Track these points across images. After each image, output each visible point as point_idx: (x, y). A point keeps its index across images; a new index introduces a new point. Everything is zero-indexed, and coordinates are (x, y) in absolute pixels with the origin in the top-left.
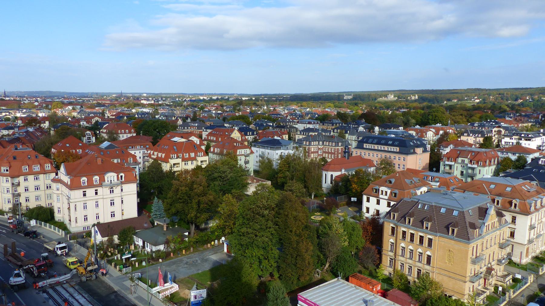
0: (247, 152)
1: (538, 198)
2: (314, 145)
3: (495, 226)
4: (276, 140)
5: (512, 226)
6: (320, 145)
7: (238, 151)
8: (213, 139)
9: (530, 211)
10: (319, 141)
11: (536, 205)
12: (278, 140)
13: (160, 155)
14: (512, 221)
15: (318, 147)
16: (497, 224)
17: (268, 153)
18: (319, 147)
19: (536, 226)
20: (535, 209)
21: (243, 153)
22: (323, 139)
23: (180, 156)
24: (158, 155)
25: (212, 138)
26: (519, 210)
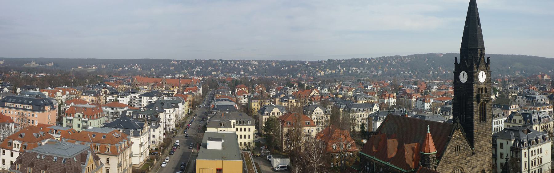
1: (122, 142)
3: (93, 168)
5: (108, 166)
9: (117, 153)
11: (121, 148)
14: (107, 162)
16: (94, 167)
19: (122, 163)
20: (121, 150)
26: (111, 153)
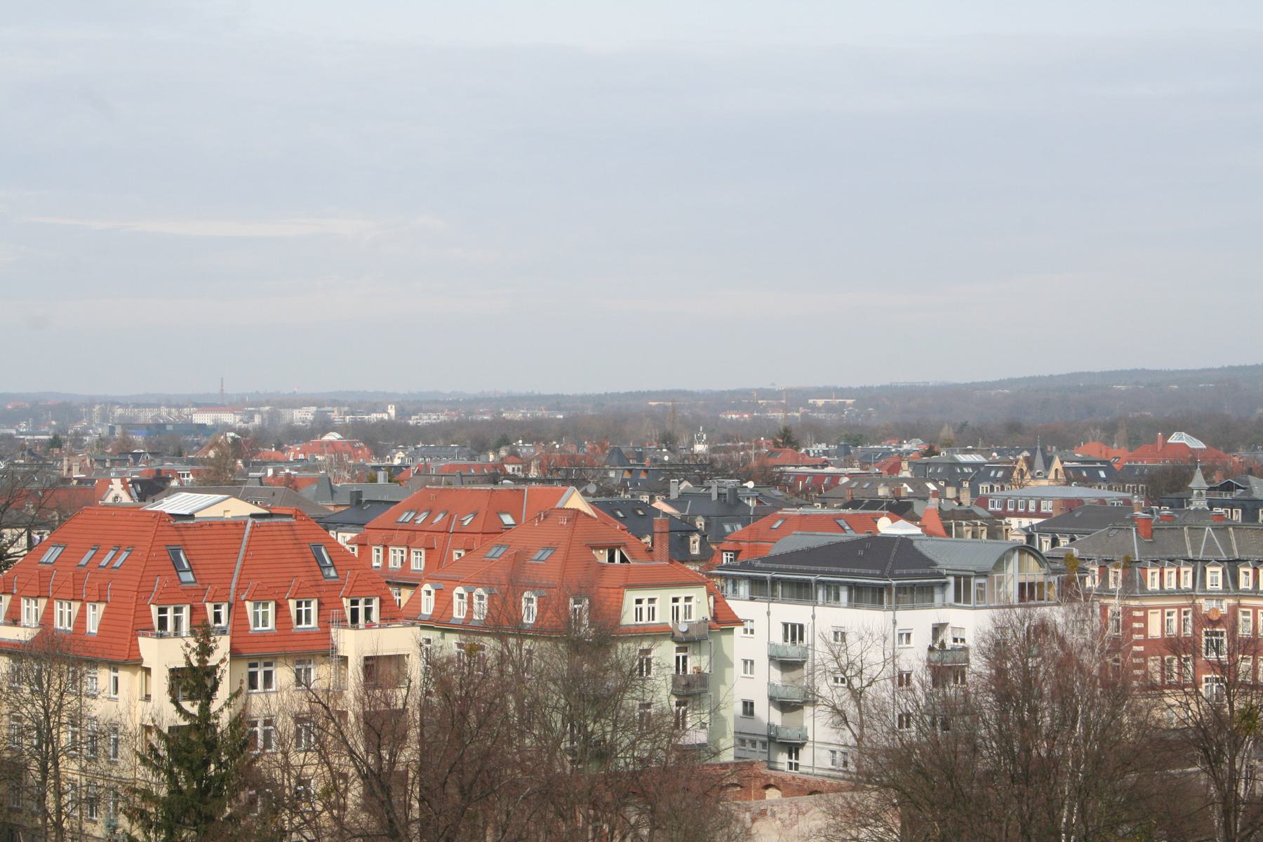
0: (688, 613)
2: (1163, 593)
4: (890, 540)
6: (1209, 596)
7: (630, 597)
8: (406, 564)
10: (1200, 566)
12: (906, 541)
13: (64, 615)
15: (1196, 609)
17: (840, 635)
18: (1206, 606)
21: (663, 616)
22: (1228, 550)
23: (217, 618)
24: (46, 620)
25: (396, 557)
